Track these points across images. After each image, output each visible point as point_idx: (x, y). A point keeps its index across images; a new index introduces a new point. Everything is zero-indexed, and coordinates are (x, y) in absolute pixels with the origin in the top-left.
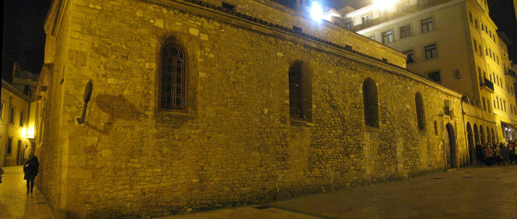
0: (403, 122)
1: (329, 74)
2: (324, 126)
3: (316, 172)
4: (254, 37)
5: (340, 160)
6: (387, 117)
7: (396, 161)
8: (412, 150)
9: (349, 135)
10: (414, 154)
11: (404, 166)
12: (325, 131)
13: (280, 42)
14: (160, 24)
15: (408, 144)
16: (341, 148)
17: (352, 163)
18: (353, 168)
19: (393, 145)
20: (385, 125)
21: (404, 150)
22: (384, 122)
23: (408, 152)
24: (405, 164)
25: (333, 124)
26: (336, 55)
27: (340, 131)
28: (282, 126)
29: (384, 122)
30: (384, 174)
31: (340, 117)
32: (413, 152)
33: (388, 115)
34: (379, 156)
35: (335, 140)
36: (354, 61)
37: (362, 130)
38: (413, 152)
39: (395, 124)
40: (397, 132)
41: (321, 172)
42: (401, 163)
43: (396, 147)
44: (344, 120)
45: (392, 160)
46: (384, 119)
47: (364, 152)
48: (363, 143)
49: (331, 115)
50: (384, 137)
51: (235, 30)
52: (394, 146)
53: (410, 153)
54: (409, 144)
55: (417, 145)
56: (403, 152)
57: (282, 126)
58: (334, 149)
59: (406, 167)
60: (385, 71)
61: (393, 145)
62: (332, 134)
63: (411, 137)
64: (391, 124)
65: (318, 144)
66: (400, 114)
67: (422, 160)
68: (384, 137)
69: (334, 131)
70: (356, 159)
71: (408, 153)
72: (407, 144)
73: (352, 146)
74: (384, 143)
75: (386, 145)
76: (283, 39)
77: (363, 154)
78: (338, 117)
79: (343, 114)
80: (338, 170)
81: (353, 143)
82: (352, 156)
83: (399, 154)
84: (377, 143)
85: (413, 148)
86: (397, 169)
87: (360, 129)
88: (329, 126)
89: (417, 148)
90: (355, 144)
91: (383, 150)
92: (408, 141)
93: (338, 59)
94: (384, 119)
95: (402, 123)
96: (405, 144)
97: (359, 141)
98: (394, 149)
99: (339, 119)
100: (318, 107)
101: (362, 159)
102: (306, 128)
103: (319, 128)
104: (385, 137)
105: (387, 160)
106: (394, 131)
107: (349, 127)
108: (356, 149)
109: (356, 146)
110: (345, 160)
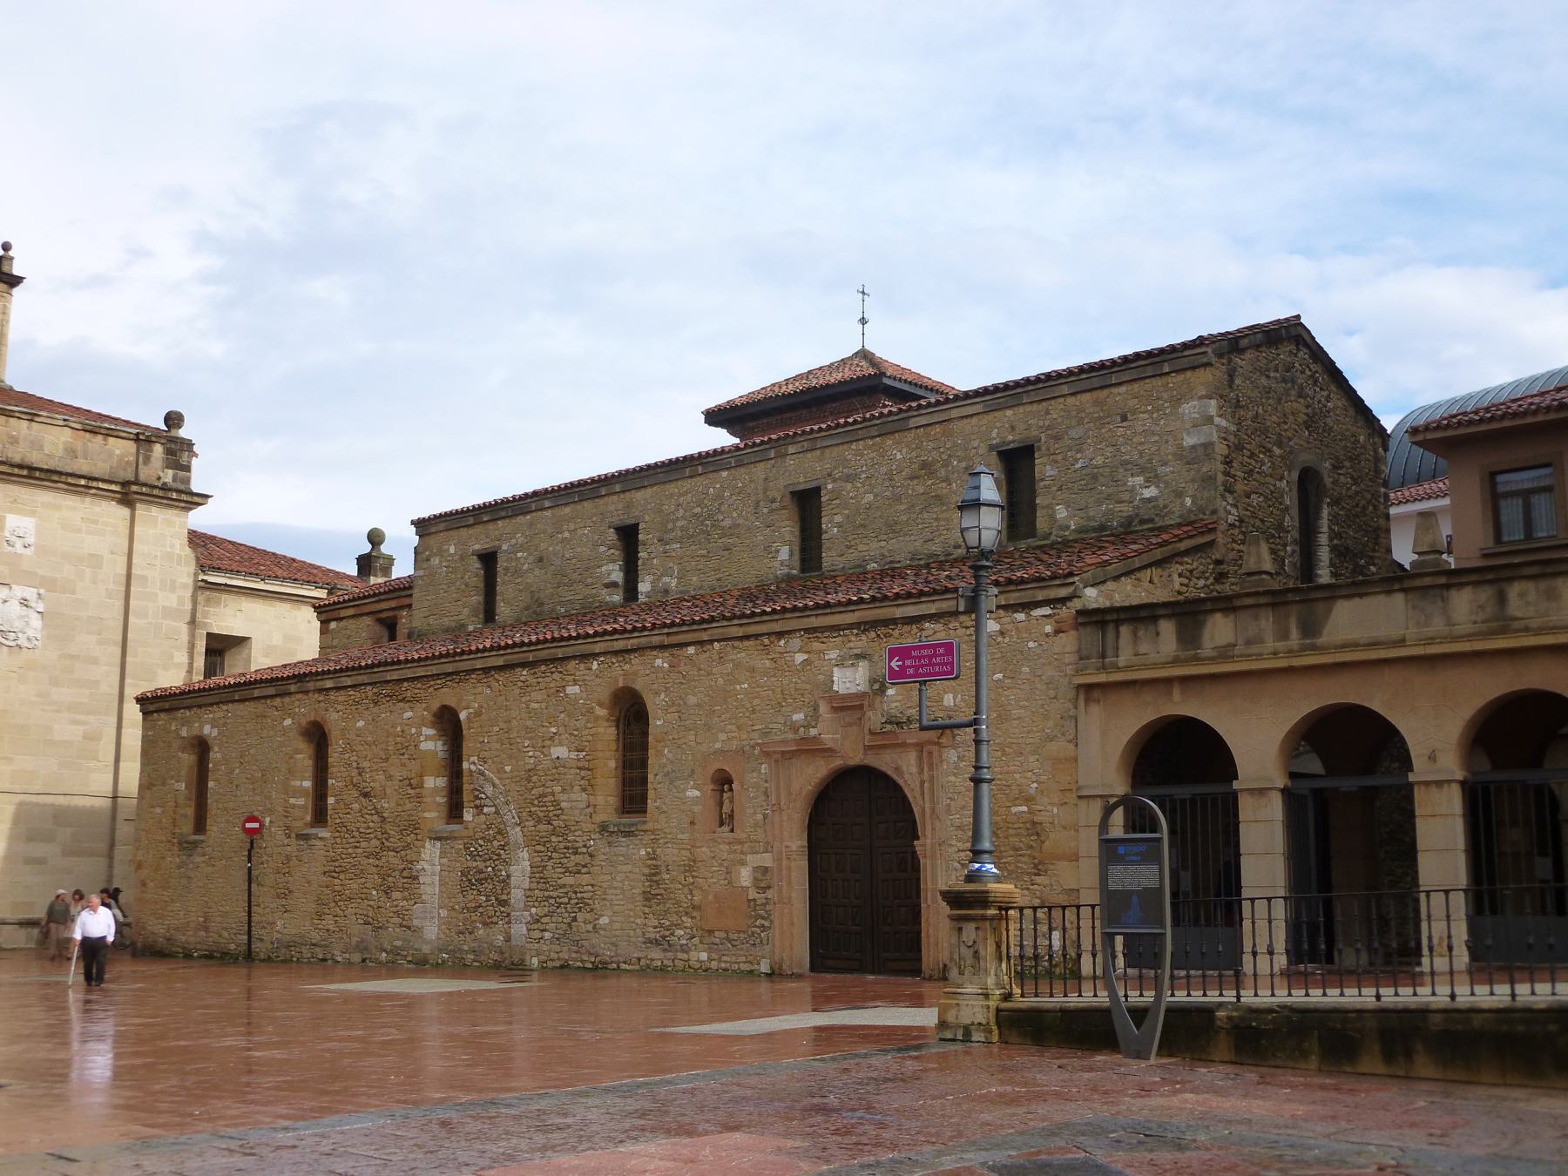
0: (536, 802)
1: (359, 729)
2: (347, 836)
3: (329, 922)
4: (259, 707)
5: (372, 903)
6: (487, 797)
7: (509, 915)
8: (564, 886)
9: (393, 851)
10: (570, 899)
11: (529, 930)
12: (348, 846)
13: (287, 700)
14: (184, 733)
15: (549, 868)
16: (376, 877)
17: (395, 909)
18: (397, 920)
19: (501, 871)
20: (483, 818)
21: (534, 886)
22: (479, 808)
23: (547, 890)
24: (536, 926)
25: (363, 830)
26: (370, 684)
27: (375, 842)
28: (286, 842)
29: (479, 808)
30: (473, 945)
31: (377, 813)
32: (564, 890)
33: (489, 790)
34: (461, 898)
35: (365, 861)
36: (407, 680)
37: (419, 837)
38: (564, 890)
39: (510, 811)
40: (516, 834)
41: (336, 922)
42: (521, 923)
43: (509, 876)
44: (384, 820)
45: (495, 912)
46: (478, 802)
47: (422, 887)
48: (419, 867)
49: (360, 811)
50: (476, 849)
51: (241, 706)
52: (504, 873)
53: (554, 894)
54: (554, 868)
55: (584, 870)
56: (530, 890)
57: (286, 842)
58: (363, 880)
59: (537, 934)
60: (486, 670)
61: (501, 871)
62: (360, 850)
63: (562, 845)
64: (497, 813)
65: (335, 872)
66: (529, 780)
67: (604, 920)
68: (476, 849)
69: (364, 844)
70: (405, 903)
71: (546, 894)
72: (545, 867)
73: (397, 873)
74: (475, 864)
75: (481, 872)
76: (290, 694)
77: (415, 891)
78: (372, 815)
79: (382, 807)
80: (369, 924)
81: (401, 867)
82: (396, 895)
83: (517, 895)
84: (458, 864)
85: (569, 880)
86: (508, 939)
87: (416, 834)
88: (356, 834)
89: (585, 879)
90: (404, 869)
91: (473, 885)
92: (550, 858)
93: (375, 690)
94: (478, 802)
95: (535, 806)
96: (538, 871)
97: (411, 862)
98: (504, 881)
99: (375, 817)
100: (337, 802)
101: (416, 903)
102: (318, 843)
103: (338, 840)
104: (480, 849)
105: (481, 910)
106: (507, 833)
107: (392, 833)
108: (405, 880)
109: (405, 874)
110: (381, 904)
